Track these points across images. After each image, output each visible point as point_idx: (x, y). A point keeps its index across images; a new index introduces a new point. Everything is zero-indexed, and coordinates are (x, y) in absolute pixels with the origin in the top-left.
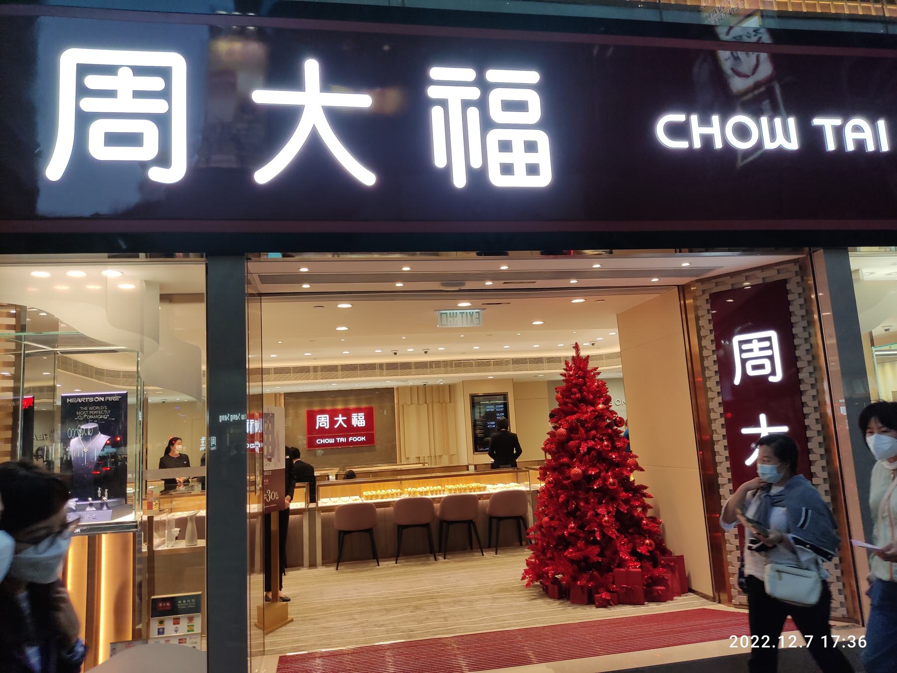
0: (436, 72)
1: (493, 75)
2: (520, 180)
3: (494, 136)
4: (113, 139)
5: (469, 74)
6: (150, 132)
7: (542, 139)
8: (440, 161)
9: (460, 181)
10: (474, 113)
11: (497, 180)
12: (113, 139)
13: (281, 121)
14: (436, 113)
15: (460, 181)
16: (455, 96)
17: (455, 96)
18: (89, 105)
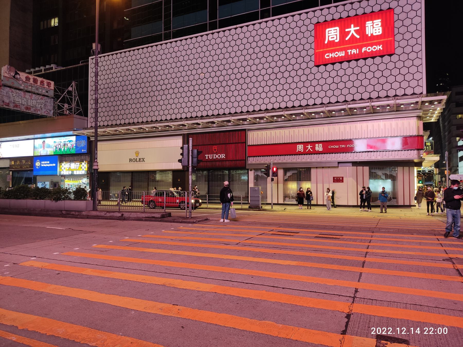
0: (367, 23)
1: (374, 21)
2: (378, 34)
3: (374, 29)
4: (331, 38)
5: (371, 22)
6: (335, 36)
7: (381, 28)
8: (367, 33)
9: (369, 35)
10: (372, 27)
11: (374, 34)
12: (331, 38)
13: (349, 32)
14: (367, 28)
15: (369, 35)
16: (369, 25)
17: (369, 25)
18: (329, 35)
